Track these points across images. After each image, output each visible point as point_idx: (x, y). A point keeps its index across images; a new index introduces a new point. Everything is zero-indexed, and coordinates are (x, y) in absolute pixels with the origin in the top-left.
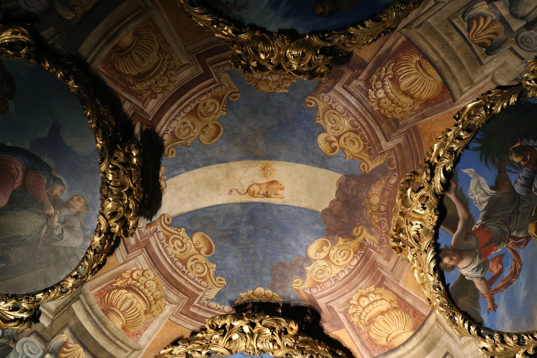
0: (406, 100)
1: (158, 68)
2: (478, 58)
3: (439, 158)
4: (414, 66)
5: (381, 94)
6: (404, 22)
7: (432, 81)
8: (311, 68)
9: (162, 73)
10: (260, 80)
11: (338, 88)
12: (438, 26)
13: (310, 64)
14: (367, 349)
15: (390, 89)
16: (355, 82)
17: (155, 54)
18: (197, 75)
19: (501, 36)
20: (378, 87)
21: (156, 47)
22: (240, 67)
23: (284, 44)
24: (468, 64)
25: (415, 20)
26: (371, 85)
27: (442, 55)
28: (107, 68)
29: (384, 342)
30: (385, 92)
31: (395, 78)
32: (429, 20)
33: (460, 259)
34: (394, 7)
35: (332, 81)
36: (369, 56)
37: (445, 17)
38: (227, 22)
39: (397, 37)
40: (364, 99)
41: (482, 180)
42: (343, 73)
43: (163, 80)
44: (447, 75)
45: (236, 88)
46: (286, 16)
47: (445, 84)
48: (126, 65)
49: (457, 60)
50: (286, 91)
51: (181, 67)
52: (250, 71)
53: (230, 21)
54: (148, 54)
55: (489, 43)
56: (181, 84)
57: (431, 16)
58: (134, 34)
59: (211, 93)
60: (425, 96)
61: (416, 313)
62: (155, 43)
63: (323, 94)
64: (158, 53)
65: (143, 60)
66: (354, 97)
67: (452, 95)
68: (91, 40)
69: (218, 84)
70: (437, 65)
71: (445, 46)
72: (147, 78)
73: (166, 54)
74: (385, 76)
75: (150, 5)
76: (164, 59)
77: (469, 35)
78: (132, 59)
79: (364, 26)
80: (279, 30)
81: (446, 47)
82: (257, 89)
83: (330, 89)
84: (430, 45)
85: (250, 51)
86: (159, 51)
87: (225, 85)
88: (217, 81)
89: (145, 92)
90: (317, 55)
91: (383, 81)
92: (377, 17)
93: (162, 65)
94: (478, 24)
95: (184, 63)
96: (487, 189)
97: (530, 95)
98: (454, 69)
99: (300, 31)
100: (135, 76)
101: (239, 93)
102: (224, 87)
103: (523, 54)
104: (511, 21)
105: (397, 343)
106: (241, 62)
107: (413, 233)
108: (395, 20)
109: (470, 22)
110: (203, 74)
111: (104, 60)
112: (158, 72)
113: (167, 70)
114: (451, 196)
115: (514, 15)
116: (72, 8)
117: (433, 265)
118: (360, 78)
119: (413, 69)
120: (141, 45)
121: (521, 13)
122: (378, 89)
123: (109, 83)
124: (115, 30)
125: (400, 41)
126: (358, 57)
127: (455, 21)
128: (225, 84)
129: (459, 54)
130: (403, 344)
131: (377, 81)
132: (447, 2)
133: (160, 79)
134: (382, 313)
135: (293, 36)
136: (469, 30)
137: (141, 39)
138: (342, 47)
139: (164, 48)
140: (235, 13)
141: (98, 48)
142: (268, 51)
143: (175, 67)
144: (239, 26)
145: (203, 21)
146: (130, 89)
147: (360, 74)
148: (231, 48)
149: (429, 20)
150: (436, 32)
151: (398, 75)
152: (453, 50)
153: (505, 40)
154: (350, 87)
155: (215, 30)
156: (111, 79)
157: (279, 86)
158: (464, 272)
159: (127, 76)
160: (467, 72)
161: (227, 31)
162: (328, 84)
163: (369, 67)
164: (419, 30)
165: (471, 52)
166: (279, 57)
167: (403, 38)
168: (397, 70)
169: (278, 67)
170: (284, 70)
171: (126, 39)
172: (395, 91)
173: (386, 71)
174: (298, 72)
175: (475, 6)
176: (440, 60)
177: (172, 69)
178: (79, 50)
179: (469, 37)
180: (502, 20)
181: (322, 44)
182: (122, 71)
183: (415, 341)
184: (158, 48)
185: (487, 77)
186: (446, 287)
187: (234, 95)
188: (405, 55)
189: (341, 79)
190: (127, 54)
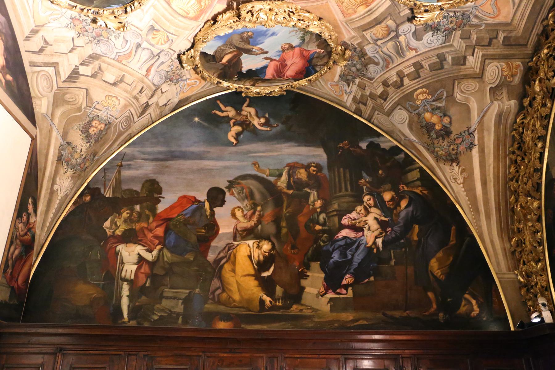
2: (156, 23)
13: (252, 15)
19: (150, 37)
27: (176, 21)
47: (169, 4)
55: (154, 32)
58: (355, 12)
68: (382, 10)
75: (344, 24)
86: (343, 3)
94: (164, 41)
97: (120, 12)
103: (133, 28)
109: (168, 40)
115: (148, 49)
116: (387, 26)
121: (146, 51)
129: (168, 24)
141: (378, 5)
150: (184, 29)
153: (147, 35)
171: (362, 10)
180: (153, 45)
185: (147, 12)
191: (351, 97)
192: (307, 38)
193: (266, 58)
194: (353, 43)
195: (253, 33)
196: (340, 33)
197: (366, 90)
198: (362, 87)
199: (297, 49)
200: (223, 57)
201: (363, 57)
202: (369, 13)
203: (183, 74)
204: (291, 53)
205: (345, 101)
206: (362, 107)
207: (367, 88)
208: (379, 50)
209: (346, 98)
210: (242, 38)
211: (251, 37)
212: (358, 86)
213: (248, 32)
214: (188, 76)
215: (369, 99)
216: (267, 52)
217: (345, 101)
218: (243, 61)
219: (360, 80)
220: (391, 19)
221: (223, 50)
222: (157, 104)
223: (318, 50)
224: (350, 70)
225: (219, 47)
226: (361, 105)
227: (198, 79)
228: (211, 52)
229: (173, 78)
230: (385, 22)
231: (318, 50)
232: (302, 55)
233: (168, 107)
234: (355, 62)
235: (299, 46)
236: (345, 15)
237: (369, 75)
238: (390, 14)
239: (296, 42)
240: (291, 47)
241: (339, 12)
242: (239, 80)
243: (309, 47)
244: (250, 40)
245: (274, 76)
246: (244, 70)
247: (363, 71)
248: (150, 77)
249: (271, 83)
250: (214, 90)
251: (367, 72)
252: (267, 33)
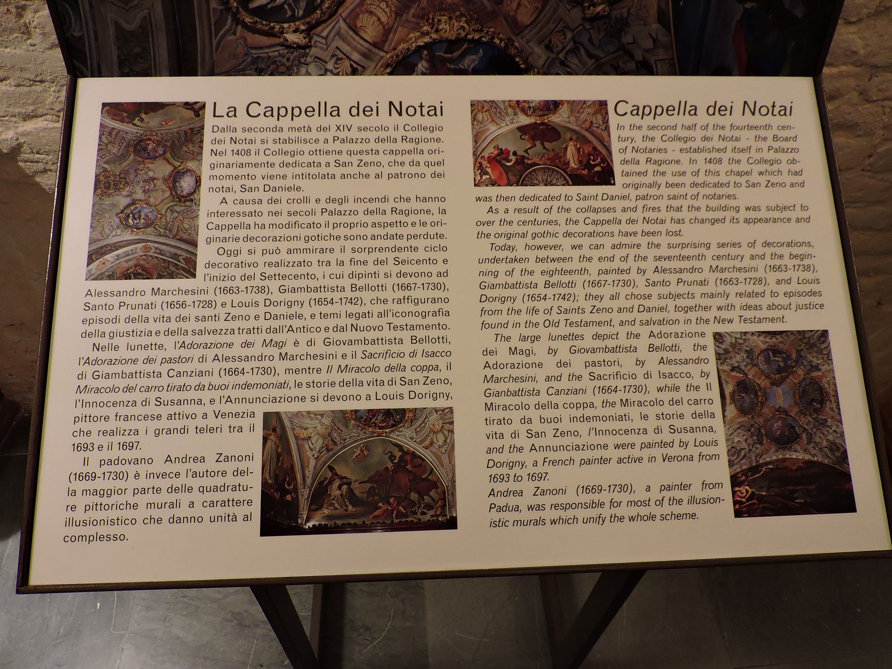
3: (487, 32)
14: (349, 14)
29: (359, 24)
33: (427, 61)
41: (477, 62)
49: (541, 30)
61: (384, 42)
96: (472, 66)
98: (535, 30)
104: (564, 52)
105: (362, 34)
107: (441, 27)
114: (465, 46)
115: (567, 53)
117: (422, 44)
130: (362, 38)
134: (379, 19)
158: (420, 65)
180: (564, 48)
183: (367, 45)
186: (409, 56)
214: (625, 10)
222: (647, 51)
233: (660, 38)
248: (602, 55)
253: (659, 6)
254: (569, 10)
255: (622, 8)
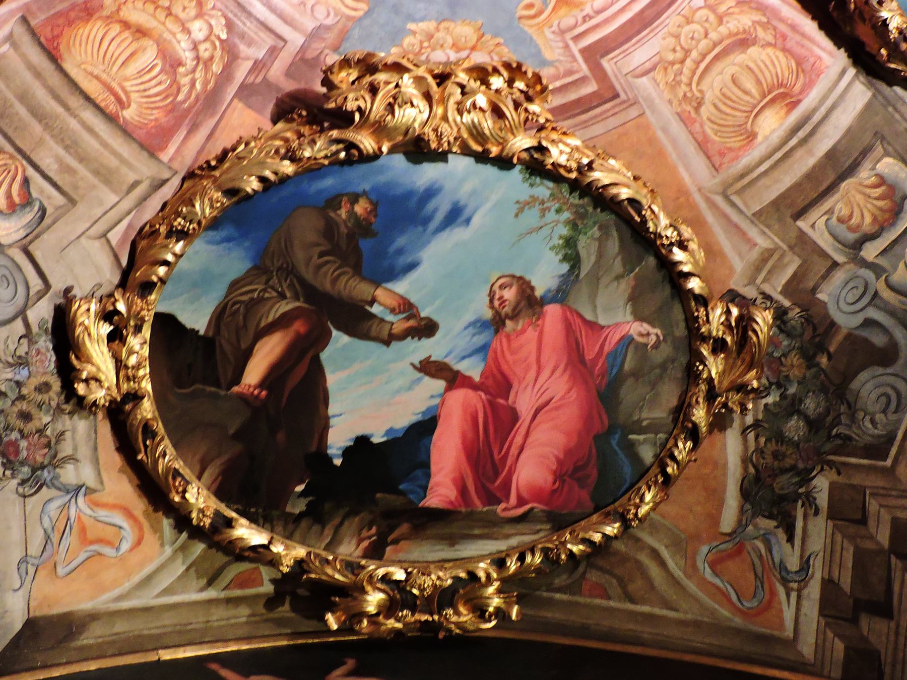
0: (136, 15)
1: (703, 66)
4: (134, 96)
5: (198, 29)
6: (167, 192)
7: (83, 63)
8: (368, 79)
9: (694, 54)
10: (473, 49)
11: (296, 40)
12: (94, 187)
13: (374, 90)
15: (179, 42)
16: (261, 54)
17: (709, 96)
18: (617, 52)
20: (207, 45)
21: (706, 111)
22: (530, 75)
23: (435, 130)
24: (11, 106)
25: (145, 198)
26: (223, 49)
27: (73, 123)
28: (812, 60)
30: (189, 32)
31: (172, 66)
32: (114, 199)
34: (199, 223)
35: (310, 55)
36: (236, 115)
37: (81, 208)
38: (562, 171)
39: (180, 159)
40: (235, 15)
42: (289, 73)
43: (692, 38)
44: (55, 79)
45: (528, 28)
46: (430, 193)
47: (54, 58)
48: (771, 67)
49: (38, 114)
50: (411, 26)
51: (653, 69)
52: (507, 66)
53: (553, 175)
54: (724, 95)
56: (652, 31)
57: (111, 208)
58: (752, 136)
59: (585, 13)
60: (95, 29)
62: (709, 119)
63: (329, 22)
64: (703, 98)
65: (734, 80)
66: (258, 20)
67: (33, 33)
69: (568, 36)
70: (82, 101)
71: (71, 145)
72: (726, 42)
73: (685, 95)
74: (194, 71)
75: (719, 200)
76: (690, 85)
77: (24, 171)
78: (758, 82)
79: (262, 179)
80: (445, 160)
81: (68, 142)
82: (479, 29)
83: (315, 35)
84: (105, 144)
85: (508, 110)
86: (700, 104)
87: (554, 32)
88: (571, 43)
89: (731, 10)
90: (359, 109)
91: (198, 58)
92: (235, 199)
93: (694, 73)
95: (644, 79)
98: (41, 95)
99: (399, 160)
100: (754, 44)
101: (520, 18)
102: (555, 28)
106: (527, 86)
108: (195, 194)
110: (603, 56)
111: (818, 76)
112: (704, 56)
113: (682, 62)
116: (882, 181)
118: (250, 64)
119: (134, 88)
120: (738, 114)
122: (206, 39)
123: (810, 26)
124: (794, 142)
125: (171, 150)
126: (259, 111)
127: (59, 199)
128: (551, 36)
129: (37, 128)
131: (212, 58)
132: (83, 239)
133: (699, 41)
135: (418, 149)
136: (26, 181)
137: (740, 126)
138: (305, 130)
139: (688, 108)
140: (544, 189)
141: (829, 103)
142: (469, 112)
143: (666, 69)
144: (536, 165)
145: (612, 170)
146: (764, 15)
147: (250, 72)
148: (550, 117)
149: (114, 199)
150: (96, 173)
151: (166, 73)
152: (52, 136)
154: (269, 41)
155: (584, 154)
156: (803, 35)
157: (430, 37)
159: (769, 44)
160: (8, 86)
161: (561, 152)
162: (318, 46)
163: (231, 90)
164: (132, 177)
165: (10, 133)
166: (444, 101)
167: (165, 156)
168: (170, 86)
169: (442, 78)
170: (431, 72)
171: (772, 125)
172: (167, 36)
173: (193, 82)
174: (398, 68)
175: (22, 233)
176: (77, 112)
177: (673, 63)
178: (869, 94)
179: (22, 165)
181: (350, 135)
182: (780, 55)
184: (703, 110)
187: (532, 12)
188: (156, 120)
189: (290, 60)
190: (770, 92)
191: (814, 590)
192: (587, 247)
193: (429, 368)
194: (767, 289)
195: (375, 205)
196: (711, 251)
197: (872, 523)
198: (848, 513)
199: (553, 311)
200: (246, 355)
201: (821, 348)
202: (801, 134)
203: (66, 449)
204: (531, 333)
205: (789, 633)
206: (873, 629)
207: (873, 506)
208: (881, 286)
209: (789, 615)
210: (330, 230)
211: (362, 228)
212: (831, 516)
213: (354, 198)
215: (893, 558)
216: (428, 329)
217: (789, 633)
218: (333, 379)
219: (833, 475)
220: (887, 154)
221: (253, 304)
223: (637, 329)
224: (780, 437)
225: (234, 285)
226: (865, 622)
227: (128, 513)
228: (197, 318)
229: (15, 444)
230: (867, 164)
231: (637, 329)
232: (576, 359)
234: (792, 390)
235: (561, 295)
236: (717, 160)
237: (869, 430)
238: (879, 136)
239: (545, 275)
240: (530, 302)
241: (691, 149)
242: (316, 516)
243: (600, 300)
244: (365, 245)
245: (463, 491)
246: (338, 439)
247: (837, 422)
249: (452, 540)
250: (198, 620)
251: (853, 418)
252: (431, 206)
253: (93, 617)
254: (104, 235)
255: (96, 461)
